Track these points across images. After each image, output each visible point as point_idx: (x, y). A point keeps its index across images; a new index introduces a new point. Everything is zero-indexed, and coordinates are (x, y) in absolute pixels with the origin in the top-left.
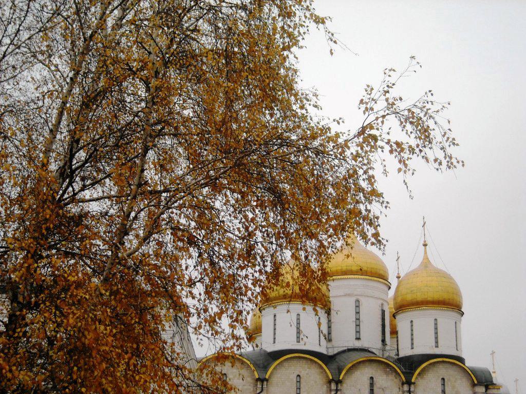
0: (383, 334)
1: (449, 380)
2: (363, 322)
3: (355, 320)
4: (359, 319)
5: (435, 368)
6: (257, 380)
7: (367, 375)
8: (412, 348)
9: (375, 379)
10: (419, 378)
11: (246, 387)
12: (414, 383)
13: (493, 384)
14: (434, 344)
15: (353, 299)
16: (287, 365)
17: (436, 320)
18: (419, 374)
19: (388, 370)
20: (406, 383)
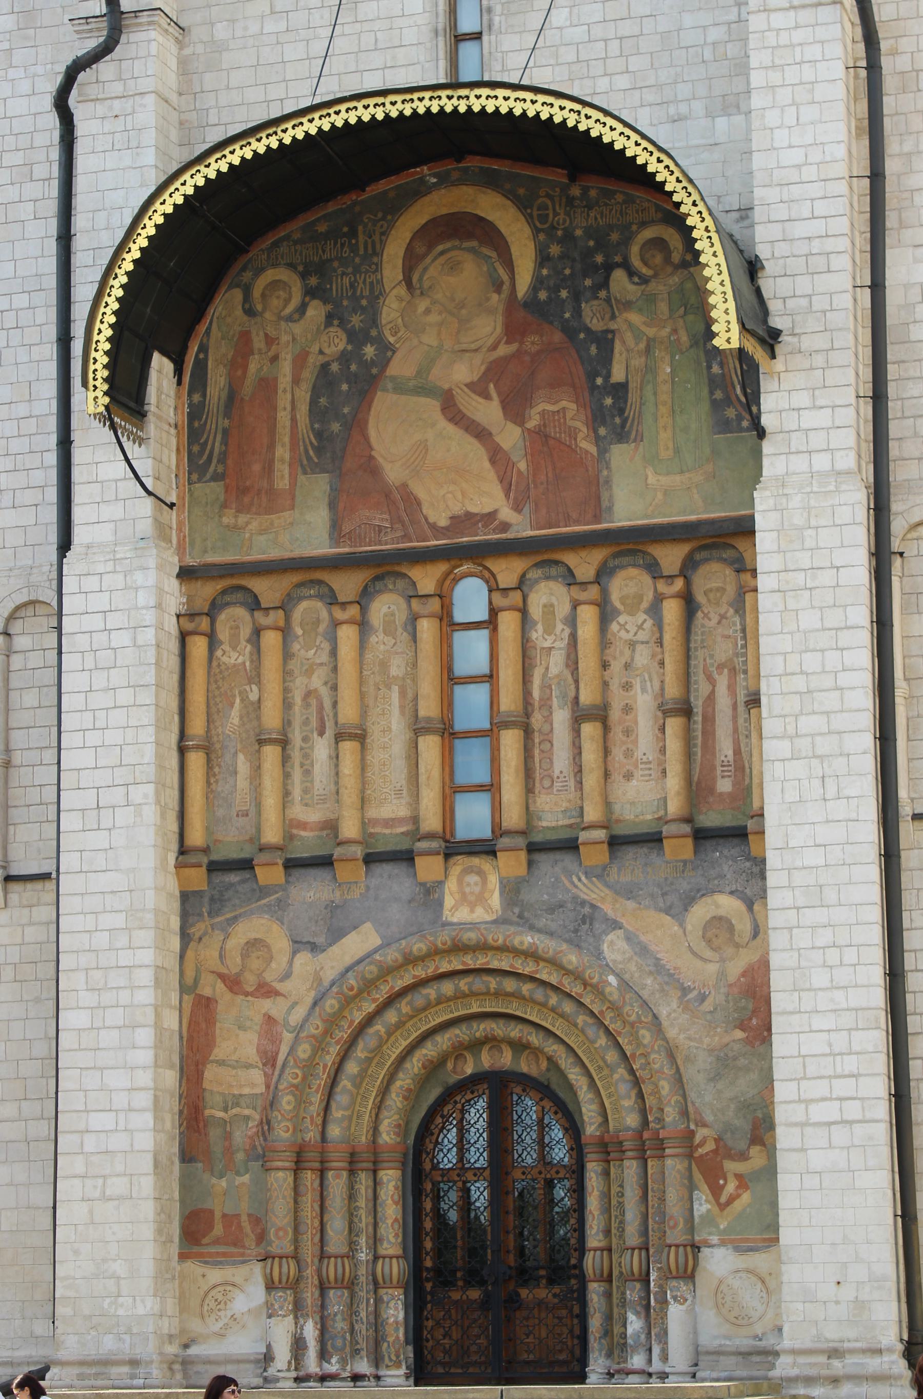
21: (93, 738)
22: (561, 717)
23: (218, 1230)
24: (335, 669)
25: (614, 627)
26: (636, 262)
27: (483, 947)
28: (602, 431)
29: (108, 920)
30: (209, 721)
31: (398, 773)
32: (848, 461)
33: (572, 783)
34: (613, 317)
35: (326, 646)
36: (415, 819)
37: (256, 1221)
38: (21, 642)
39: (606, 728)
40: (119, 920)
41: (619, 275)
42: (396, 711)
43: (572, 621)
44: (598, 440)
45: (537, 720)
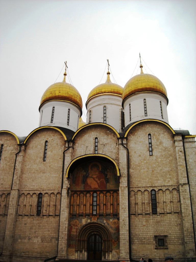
1: (154, 135)
2: (108, 118)
3: (103, 117)
5: (143, 128)
6: (18, 145)
7: (93, 137)
8: (130, 120)
9: (98, 139)
10: (131, 136)
11: (13, 151)
13: (189, 135)
16: (40, 135)
17: (145, 99)
18: (131, 132)
19: (108, 132)
20: (120, 138)
21: (64, 204)
22: (102, 205)
23: (72, 246)
24: (84, 200)
25: (107, 198)
26: (109, 169)
27: (95, 223)
28: (106, 182)
30: (73, 204)
31: (89, 208)
33: (103, 210)
34: (107, 173)
35: (83, 198)
36: (90, 212)
37: (75, 245)
38: (58, 196)
39: (106, 206)
40: (65, 219)
41: (108, 170)
43: (103, 197)
44: (106, 182)
45: (100, 205)
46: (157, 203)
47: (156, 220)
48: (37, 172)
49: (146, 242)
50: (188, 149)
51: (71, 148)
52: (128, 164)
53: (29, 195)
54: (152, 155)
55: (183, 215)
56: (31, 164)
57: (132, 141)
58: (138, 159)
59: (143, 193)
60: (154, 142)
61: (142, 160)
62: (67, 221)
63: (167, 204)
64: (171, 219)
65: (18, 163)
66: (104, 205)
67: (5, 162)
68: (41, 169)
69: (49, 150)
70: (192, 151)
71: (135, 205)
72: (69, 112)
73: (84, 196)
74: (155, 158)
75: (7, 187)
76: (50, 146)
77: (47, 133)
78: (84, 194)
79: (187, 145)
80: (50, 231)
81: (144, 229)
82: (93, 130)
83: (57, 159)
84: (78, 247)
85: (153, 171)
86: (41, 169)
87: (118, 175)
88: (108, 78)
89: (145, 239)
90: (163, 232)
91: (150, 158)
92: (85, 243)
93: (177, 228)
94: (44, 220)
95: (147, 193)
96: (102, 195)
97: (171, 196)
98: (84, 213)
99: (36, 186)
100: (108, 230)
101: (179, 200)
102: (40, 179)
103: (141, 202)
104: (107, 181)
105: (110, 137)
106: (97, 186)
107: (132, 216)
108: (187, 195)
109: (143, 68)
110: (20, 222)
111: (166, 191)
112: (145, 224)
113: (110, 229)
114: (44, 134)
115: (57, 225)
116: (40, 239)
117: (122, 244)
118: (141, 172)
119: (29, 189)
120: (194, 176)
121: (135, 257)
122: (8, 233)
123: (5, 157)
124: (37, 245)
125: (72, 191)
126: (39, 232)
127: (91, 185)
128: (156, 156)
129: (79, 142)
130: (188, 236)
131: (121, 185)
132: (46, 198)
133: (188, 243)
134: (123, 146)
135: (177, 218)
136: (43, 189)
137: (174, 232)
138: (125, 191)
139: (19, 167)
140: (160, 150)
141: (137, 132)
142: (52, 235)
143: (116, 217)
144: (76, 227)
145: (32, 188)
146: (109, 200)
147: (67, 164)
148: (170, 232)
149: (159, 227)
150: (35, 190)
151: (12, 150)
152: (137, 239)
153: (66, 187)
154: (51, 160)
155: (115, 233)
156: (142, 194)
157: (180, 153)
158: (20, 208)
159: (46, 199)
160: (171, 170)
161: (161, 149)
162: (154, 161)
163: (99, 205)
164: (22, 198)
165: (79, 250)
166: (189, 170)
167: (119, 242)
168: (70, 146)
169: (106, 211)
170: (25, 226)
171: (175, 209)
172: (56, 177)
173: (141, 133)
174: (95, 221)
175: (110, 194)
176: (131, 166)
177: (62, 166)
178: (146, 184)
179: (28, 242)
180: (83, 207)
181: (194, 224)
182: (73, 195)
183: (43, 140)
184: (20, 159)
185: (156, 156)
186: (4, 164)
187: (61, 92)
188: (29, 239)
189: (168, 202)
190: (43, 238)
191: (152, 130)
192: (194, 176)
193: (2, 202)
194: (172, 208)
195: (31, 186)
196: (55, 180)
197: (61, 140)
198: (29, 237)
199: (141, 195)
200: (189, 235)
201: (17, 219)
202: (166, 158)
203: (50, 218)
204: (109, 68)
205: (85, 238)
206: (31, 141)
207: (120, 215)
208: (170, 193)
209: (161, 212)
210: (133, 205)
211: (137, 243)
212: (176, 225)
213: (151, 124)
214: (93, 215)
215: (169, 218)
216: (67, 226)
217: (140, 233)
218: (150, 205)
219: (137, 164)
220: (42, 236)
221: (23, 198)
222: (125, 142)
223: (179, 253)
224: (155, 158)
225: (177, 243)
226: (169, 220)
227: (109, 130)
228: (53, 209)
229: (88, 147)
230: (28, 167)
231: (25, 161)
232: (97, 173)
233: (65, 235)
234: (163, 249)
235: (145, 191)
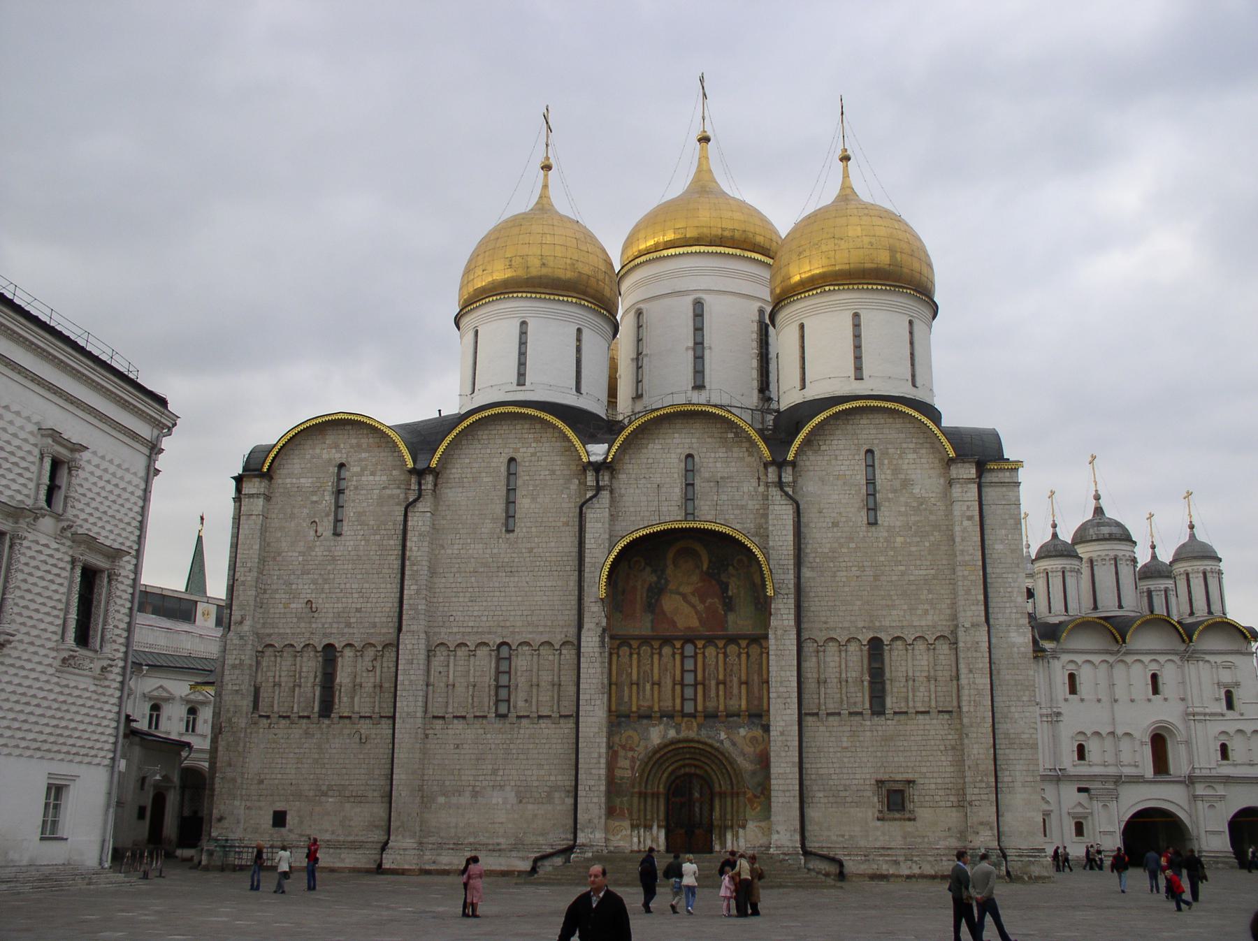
0: (762, 376)
1: (885, 453)
2: (710, 348)
3: (691, 344)
4: (702, 343)
5: (849, 427)
6: (412, 471)
7: (679, 451)
8: (803, 387)
10: (810, 453)
11: (388, 492)
12: (794, 464)
13: (999, 457)
14: (851, 373)
15: (687, 303)
16: (484, 437)
18: (808, 442)
19: (731, 435)
21: (589, 681)
22: (713, 683)
23: (618, 811)
27: (692, 741)
28: (725, 608)
29: (593, 730)
32: (792, 623)
35: (650, 659)
36: (674, 707)
37: (628, 809)
38: (564, 652)
39: (725, 686)
40: (597, 730)
41: (731, 568)
42: (669, 677)
45: (707, 682)
46: (888, 682)
47: (880, 733)
48: (486, 570)
49: (849, 799)
50: (993, 507)
51: (604, 490)
52: (796, 551)
53: (463, 648)
54: (875, 523)
55: (965, 721)
56: (462, 541)
57: (812, 473)
58: (830, 535)
59: (842, 647)
60: (881, 478)
61: (842, 541)
62: (605, 734)
63: (917, 684)
64: (929, 730)
65: (415, 539)
66: (718, 684)
67: (362, 533)
68: (501, 560)
69: (524, 493)
70: (1007, 517)
71: (817, 686)
72: (579, 340)
73: (652, 654)
74: (886, 534)
75: (377, 620)
76: (528, 478)
77: (511, 427)
78: (652, 648)
79: (991, 494)
80: (545, 767)
81: (846, 760)
82: (678, 426)
83: (553, 524)
84: (639, 816)
85: (876, 578)
86: (501, 560)
87: (770, 592)
88: (703, 158)
89: (846, 790)
90: (902, 770)
91: (870, 534)
92: (658, 801)
93: (943, 758)
94: (522, 731)
95: (857, 649)
96: (711, 651)
97: (931, 659)
98: (656, 708)
99: (484, 619)
100: (732, 762)
101: (954, 674)
102: (498, 594)
103: (838, 675)
104: (729, 605)
105: (735, 455)
106: (695, 623)
107: (810, 719)
108: (979, 660)
109: (849, 163)
110: (439, 741)
111: (915, 643)
112: (849, 744)
113: (740, 760)
114: (503, 432)
115: (566, 746)
116: (513, 794)
117: (780, 805)
118: (837, 579)
119: (462, 630)
120: (1005, 600)
121: (817, 845)
122: (403, 777)
123: (360, 514)
124: (504, 811)
125: (612, 637)
126: (506, 772)
127: (675, 618)
128: (889, 526)
129: (630, 466)
130: (977, 785)
131: (773, 622)
132: (524, 658)
133: (977, 803)
134: (782, 489)
135: (946, 727)
136: (511, 629)
137: (936, 769)
138: (787, 642)
139: (419, 554)
140: (903, 509)
141: (827, 442)
142: (553, 778)
143: (756, 721)
144: (630, 754)
145: (471, 624)
146: (735, 668)
147: (594, 546)
148: (924, 770)
149: (890, 754)
150: (483, 633)
151: (384, 488)
152: (824, 790)
153: (593, 626)
154: (534, 529)
155: (754, 773)
156: (840, 651)
157: (966, 523)
158: (434, 692)
159: (524, 663)
160: (935, 577)
161: (907, 504)
162: (880, 545)
163: (704, 684)
164: (436, 659)
165: (642, 824)
166: (991, 578)
167: (769, 798)
168: (601, 483)
169: (725, 703)
170: (457, 751)
171: (942, 699)
172: (553, 588)
173: (841, 447)
174: (692, 734)
175: (740, 647)
176: (806, 559)
177: (576, 550)
178: (853, 618)
179: (472, 803)
180: (652, 689)
181: (997, 747)
182: (616, 651)
183: (499, 455)
184: (418, 521)
185: (890, 529)
186: (359, 537)
187: (551, 264)
188: (475, 794)
189: (921, 679)
190: (522, 789)
191: (880, 436)
192: (1005, 600)
193: (365, 674)
194: (933, 697)
195: (467, 618)
196: (551, 598)
197: (563, 458)
198: (474, 786)
199: (837, 654)
200: (981, 781)
201: (427, 732)
202: (920, 534)
203: (543, 726)
204: (706, 115)
205: (658, 788)
206: (455, 456)
207: (772, 718)
208: (929, 649)
209: (897, 710)
210: (810, 685)
211: (822, 800)
212: (942, 748)
213: (876, 416)
214: (684, 715)
215: (922, 727)
216: (603, 750)
217: (832, 771)
218: (863, 687)
219: (827, 551)
220: (519, 784)
221: (442, 658)
222: (787, 477)
223: (947, 834)
224: (886, 534)
225: (942, 804)
226: (922, 732)
227: (734, 430)
228: (553, 697)
229: (661, 485)
230: (449, 551)
231: (438, 530)
232: (695, 578)
233: (599, 779)
234: (900, 819)
235: (848, 641)
